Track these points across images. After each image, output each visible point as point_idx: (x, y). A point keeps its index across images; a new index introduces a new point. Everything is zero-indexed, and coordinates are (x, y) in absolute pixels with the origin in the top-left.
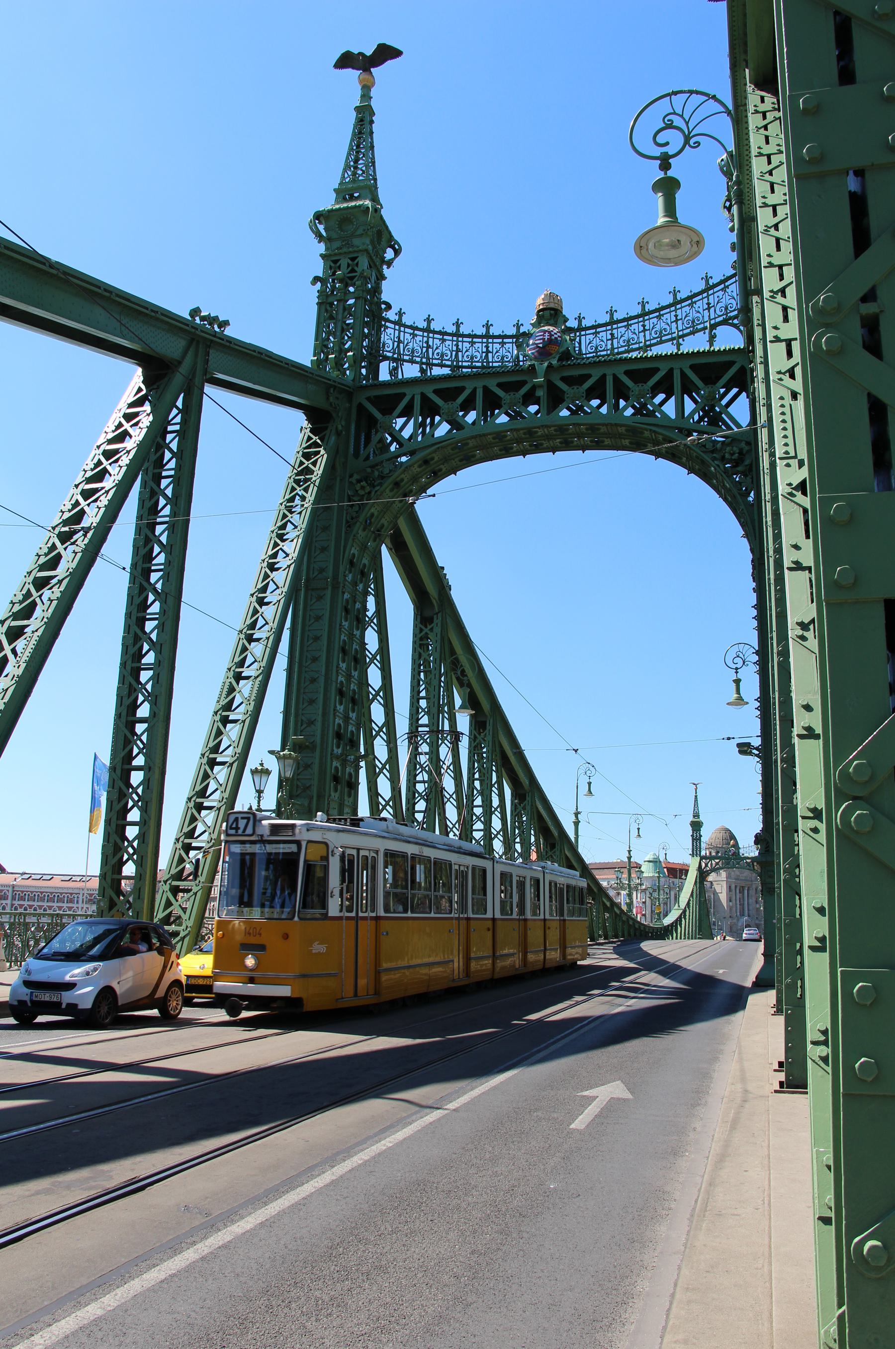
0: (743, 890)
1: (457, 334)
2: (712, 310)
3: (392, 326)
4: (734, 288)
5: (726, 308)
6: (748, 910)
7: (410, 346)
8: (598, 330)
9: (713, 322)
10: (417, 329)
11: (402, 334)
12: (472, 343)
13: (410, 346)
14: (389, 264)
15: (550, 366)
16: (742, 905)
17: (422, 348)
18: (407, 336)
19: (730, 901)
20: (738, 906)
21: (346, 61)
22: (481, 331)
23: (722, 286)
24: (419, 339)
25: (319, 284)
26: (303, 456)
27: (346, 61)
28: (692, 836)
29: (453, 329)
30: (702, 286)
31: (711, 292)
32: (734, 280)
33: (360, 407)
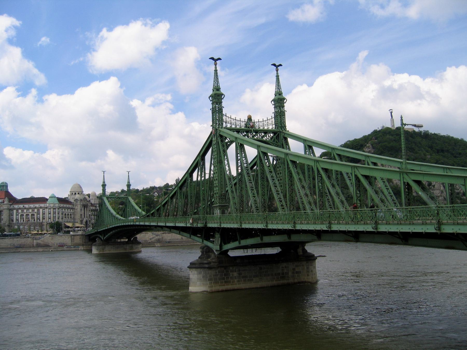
1: (236, 120)
15: (254, 130)
16: (84, 213)
29: (235, 119)
30: (271, 118)
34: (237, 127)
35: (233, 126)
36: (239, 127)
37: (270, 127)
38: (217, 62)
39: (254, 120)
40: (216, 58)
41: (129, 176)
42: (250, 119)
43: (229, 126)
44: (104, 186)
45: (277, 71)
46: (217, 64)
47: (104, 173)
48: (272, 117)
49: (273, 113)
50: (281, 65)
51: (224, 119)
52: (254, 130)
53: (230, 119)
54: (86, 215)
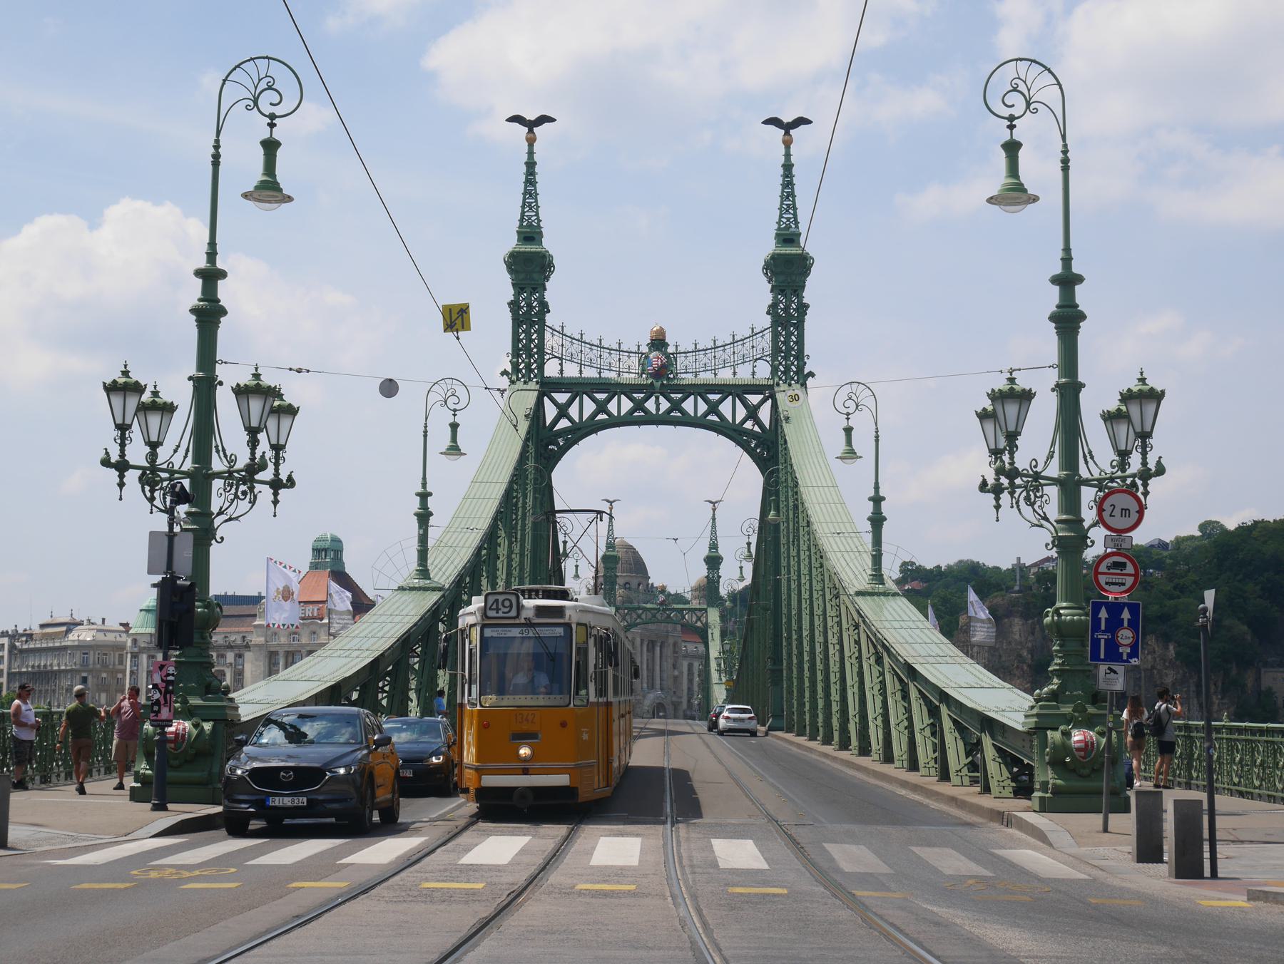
2: (755, 349)
3: (557, 334)
4: (768, 336)
5: (763, 349)
6: (661, 680)
9: (755, 358)
11: (564, 341)
12: (610, 354)
13: (570, 350)
15: (662, 384)
17: (578, 353)
18: (568, 343)
21: (516, 119)
22: (616, 347)
23: (761, 334)
24: (575, 346)
27: (516, 119)
32: (768, 331)
34: (606, 374)
35: (590, 373)
38: (535, 129)
39: (677, 346)
40: (531, 116)
42: (658, 342)
43: (571, 371)
45: (787, 144)
46: (535, 140)
48: (753, 329)
49: (768, 313)
52: (662, 384)
53: (577, 346)
54: (658, 682)
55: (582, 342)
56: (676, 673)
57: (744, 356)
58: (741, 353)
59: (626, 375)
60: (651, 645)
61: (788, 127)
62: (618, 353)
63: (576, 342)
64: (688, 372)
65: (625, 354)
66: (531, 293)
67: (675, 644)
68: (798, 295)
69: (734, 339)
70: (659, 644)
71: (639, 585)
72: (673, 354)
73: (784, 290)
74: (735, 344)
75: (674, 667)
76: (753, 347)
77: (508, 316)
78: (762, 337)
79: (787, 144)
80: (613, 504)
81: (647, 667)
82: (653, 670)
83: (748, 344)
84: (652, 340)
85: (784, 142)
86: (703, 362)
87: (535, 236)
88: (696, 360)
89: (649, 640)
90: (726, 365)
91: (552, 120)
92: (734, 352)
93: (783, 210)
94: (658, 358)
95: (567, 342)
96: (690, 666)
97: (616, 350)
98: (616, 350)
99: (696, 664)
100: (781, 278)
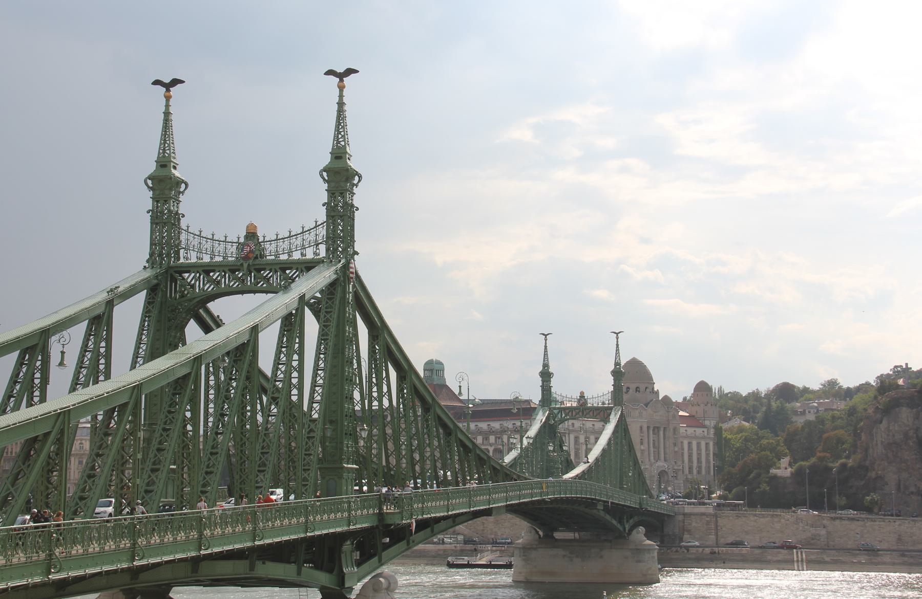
0: (658, 431)
7: (193, 243)
8: (272, 242)
10: (196, 235)
12: (219, 244)
14: (183, 193)
15: (249, 265)
19: (642, 443)
20: (652, 449)
22: (223, 239)
25: (151, 212)
26: (148, 303)
28: (542, 386)
29: (210, 237)
31: (317, 228)
32: (325, 224)
33: (172, 276)
34: (218, 259)
35: (206, 259)
36: (221, 259)
37: (310, 255)
39: (264, 237)
41: (617, 345)
42: (251, 235)
44: (546, 375)
45: (341, 88)
47: (546, 340)
48: (316, 222)
50: (350, 72)
51: (183, 241)
53: (197, 239)
55: (201, 237)
56: (676, 449)
57: (310, 242)
58: (308, 240)
59: (230, 259)
60: (656, 430)
61: (341, 76)
62: (225, 243)
63: (197, 237)
64: (272, 255)
65: (229, 244)
66: (164, 204)
67: (675, 429)
68: (344, 196)
69: (303, 230)
70: (662, 429)
71: (646, 388)
72: (262, 242)
73: (334, 193)
74: (304, 234)
75: (675, 445)
76: (316, 235)
77: (146, 221)
78: (324, 226)
79: (341, 88)
80: (547, 336)
81: (654, 444)
82: (659, 448)
83: (313, 233)
84: (247, 233)
85: (339, 87)
86: (282, 247)
87: (167, 163)
88: (277, 246)
89: (654, 428)
90: (298, 249)
91: (182, 82)
92: (303, 240)
93: (336, 138)
94: (248, 246)
95: (191, 237)
96: (690, 444)
97: (223, 242)
98: (223, 242)
99: (694, 443)
100: (333, 184)
